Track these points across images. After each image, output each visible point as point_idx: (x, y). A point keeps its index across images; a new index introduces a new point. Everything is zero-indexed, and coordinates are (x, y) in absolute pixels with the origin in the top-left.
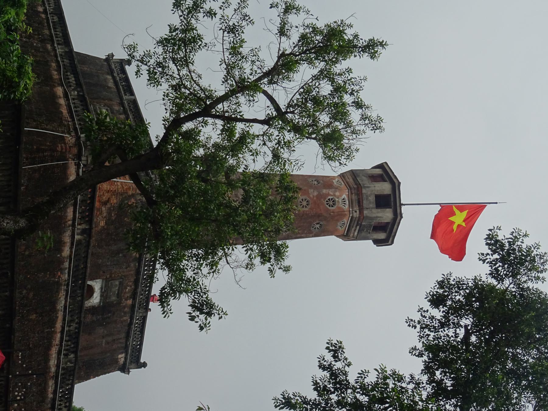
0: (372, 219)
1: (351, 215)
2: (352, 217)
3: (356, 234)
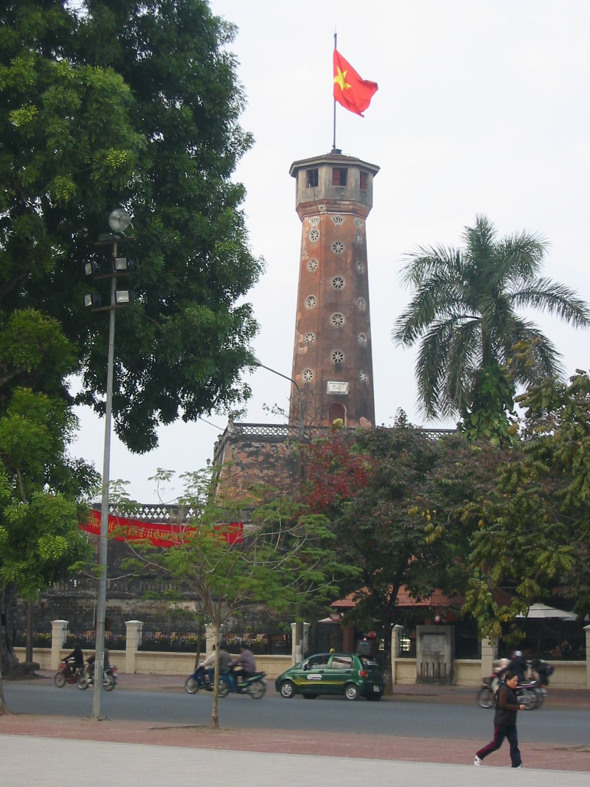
0: (327, 190)
1: (325, 212)
2: (327, 211)
3: (348, 203)
